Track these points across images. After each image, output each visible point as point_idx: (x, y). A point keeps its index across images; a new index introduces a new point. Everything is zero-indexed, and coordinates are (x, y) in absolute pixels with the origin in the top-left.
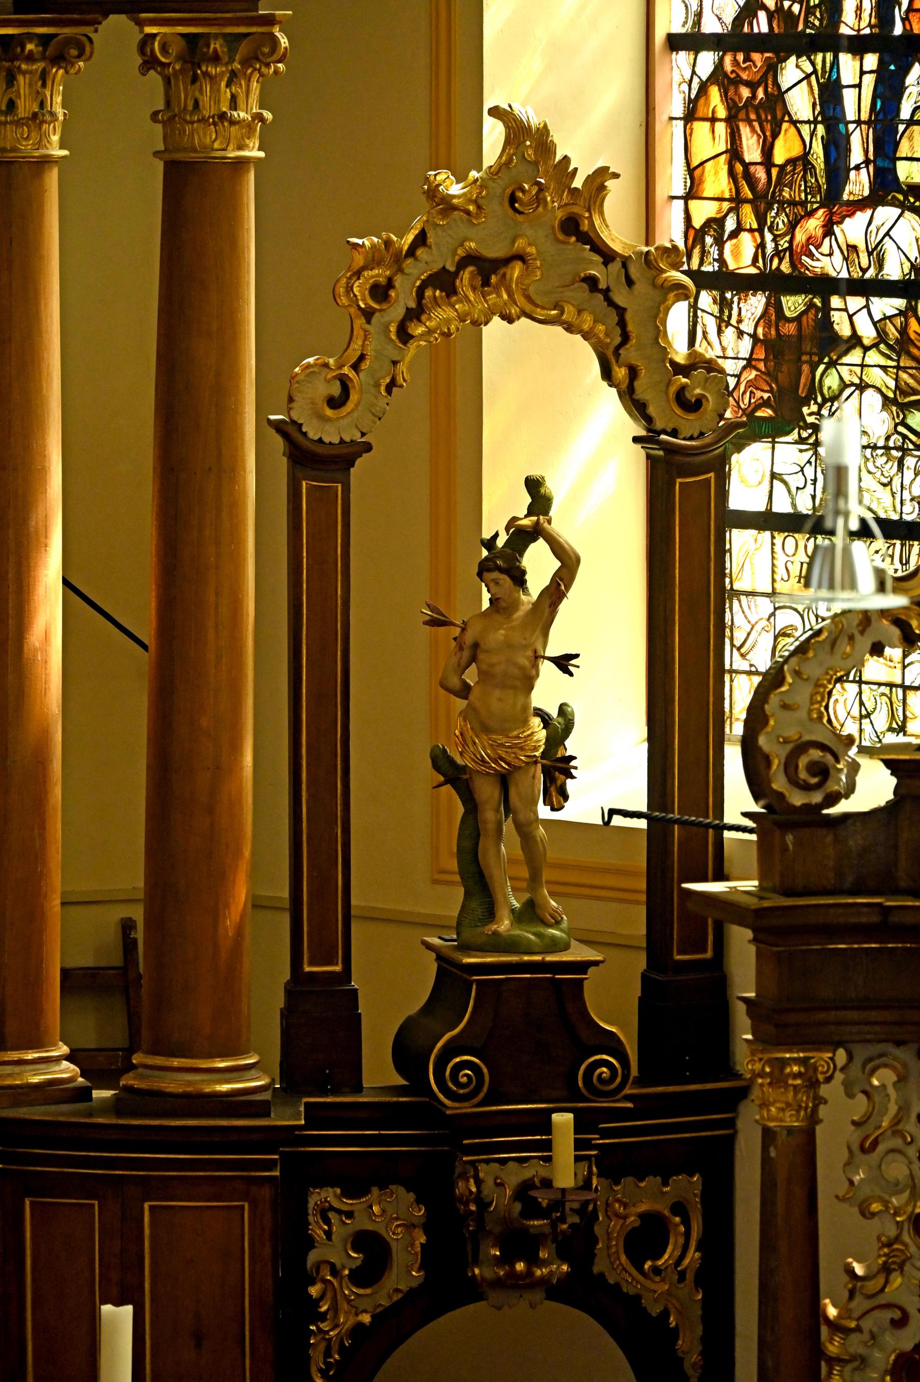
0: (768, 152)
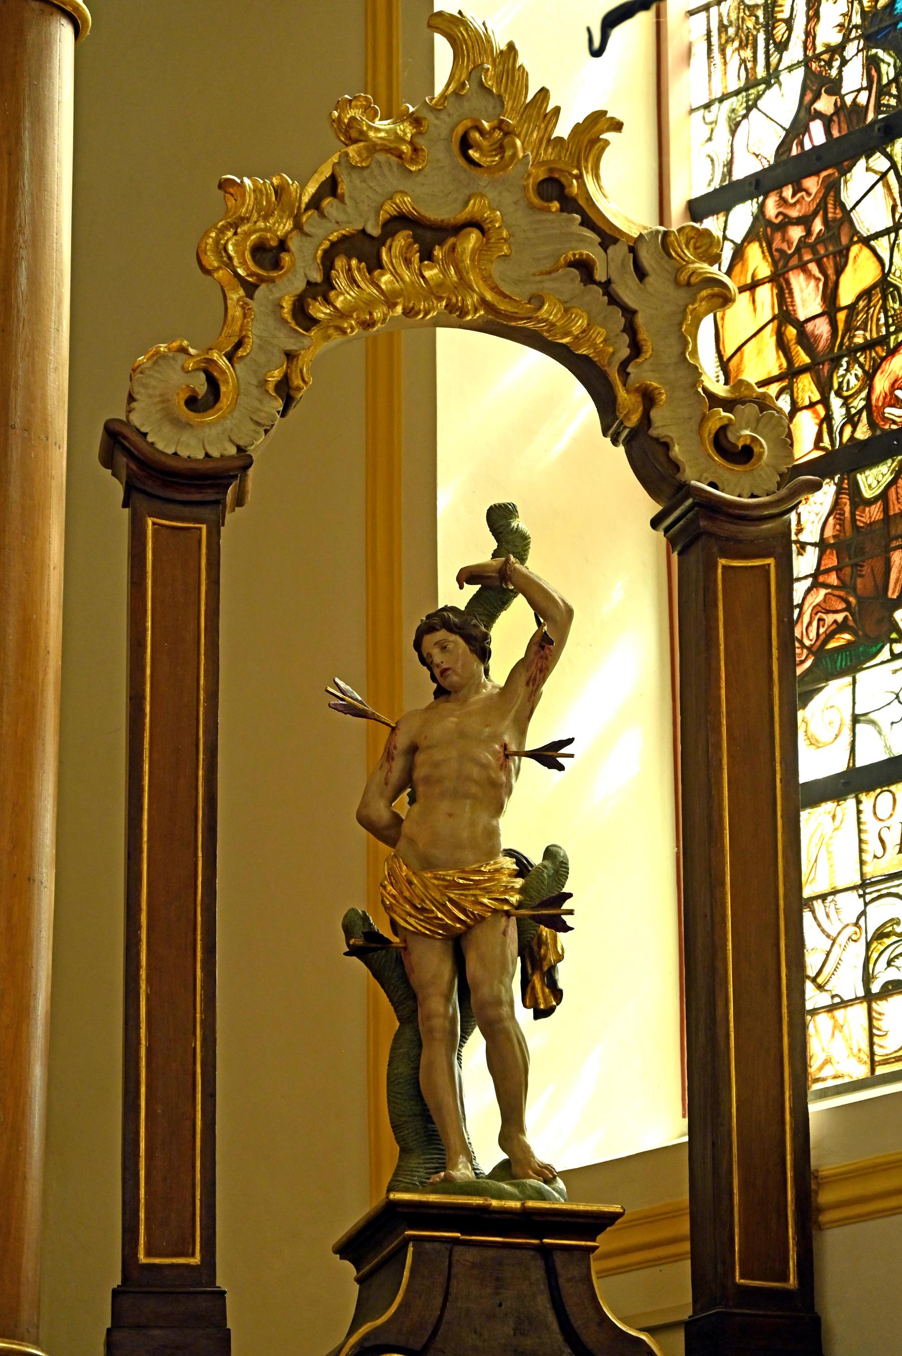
0: (830, 296)
